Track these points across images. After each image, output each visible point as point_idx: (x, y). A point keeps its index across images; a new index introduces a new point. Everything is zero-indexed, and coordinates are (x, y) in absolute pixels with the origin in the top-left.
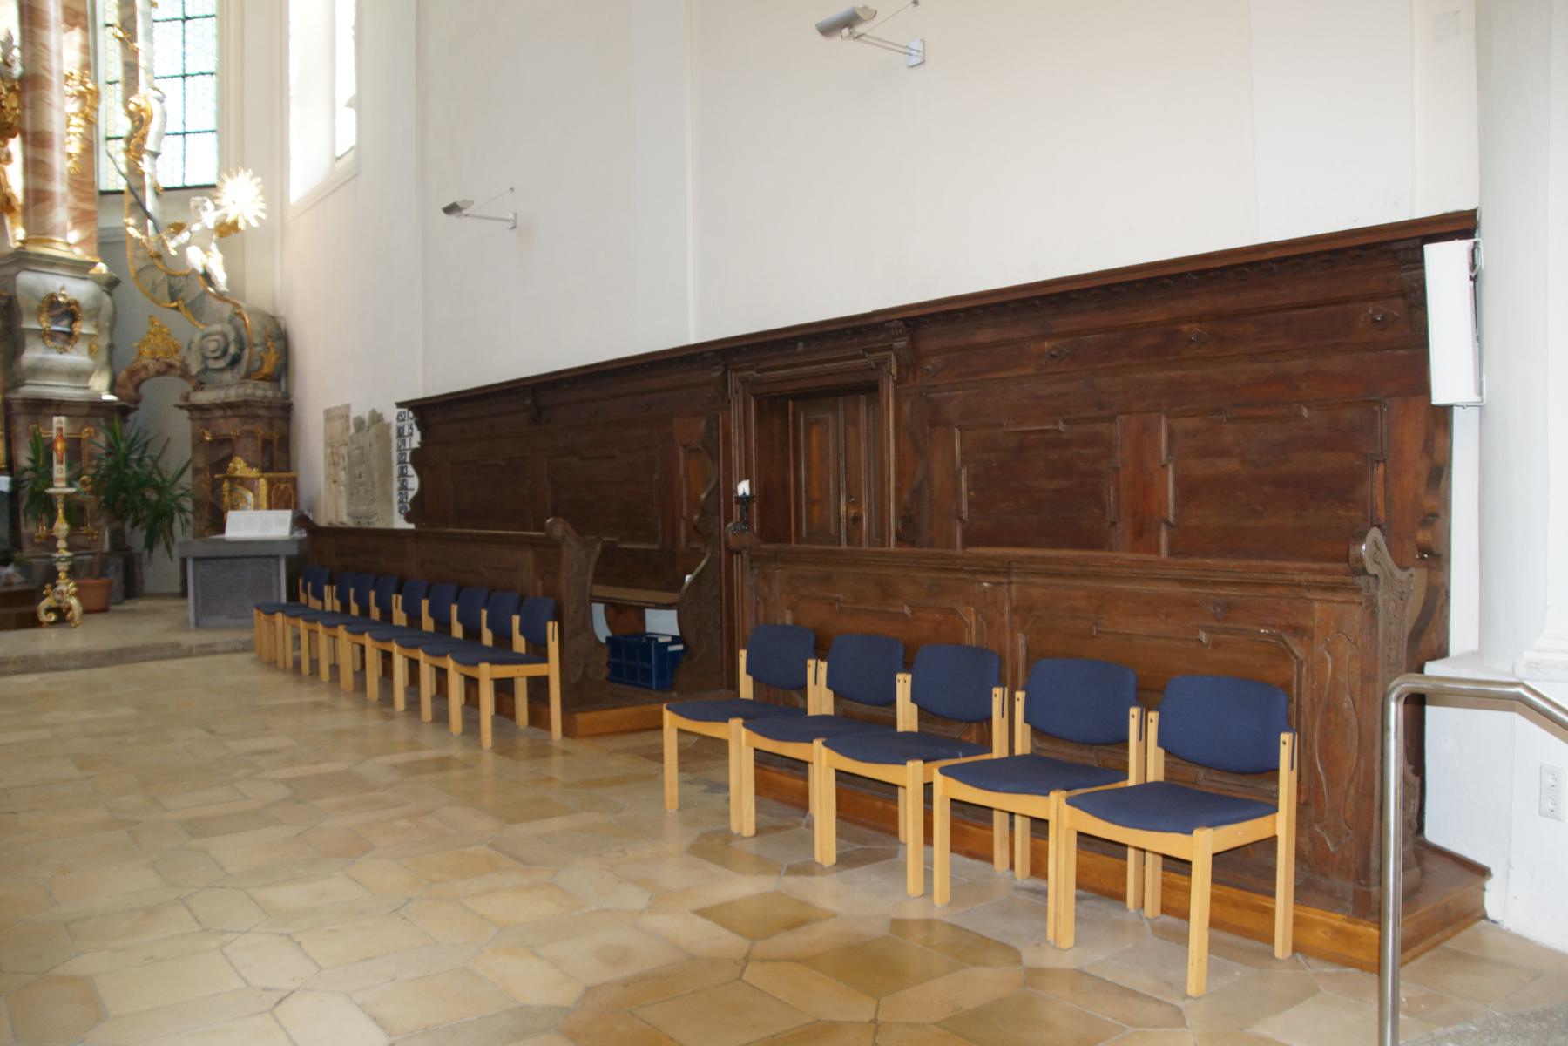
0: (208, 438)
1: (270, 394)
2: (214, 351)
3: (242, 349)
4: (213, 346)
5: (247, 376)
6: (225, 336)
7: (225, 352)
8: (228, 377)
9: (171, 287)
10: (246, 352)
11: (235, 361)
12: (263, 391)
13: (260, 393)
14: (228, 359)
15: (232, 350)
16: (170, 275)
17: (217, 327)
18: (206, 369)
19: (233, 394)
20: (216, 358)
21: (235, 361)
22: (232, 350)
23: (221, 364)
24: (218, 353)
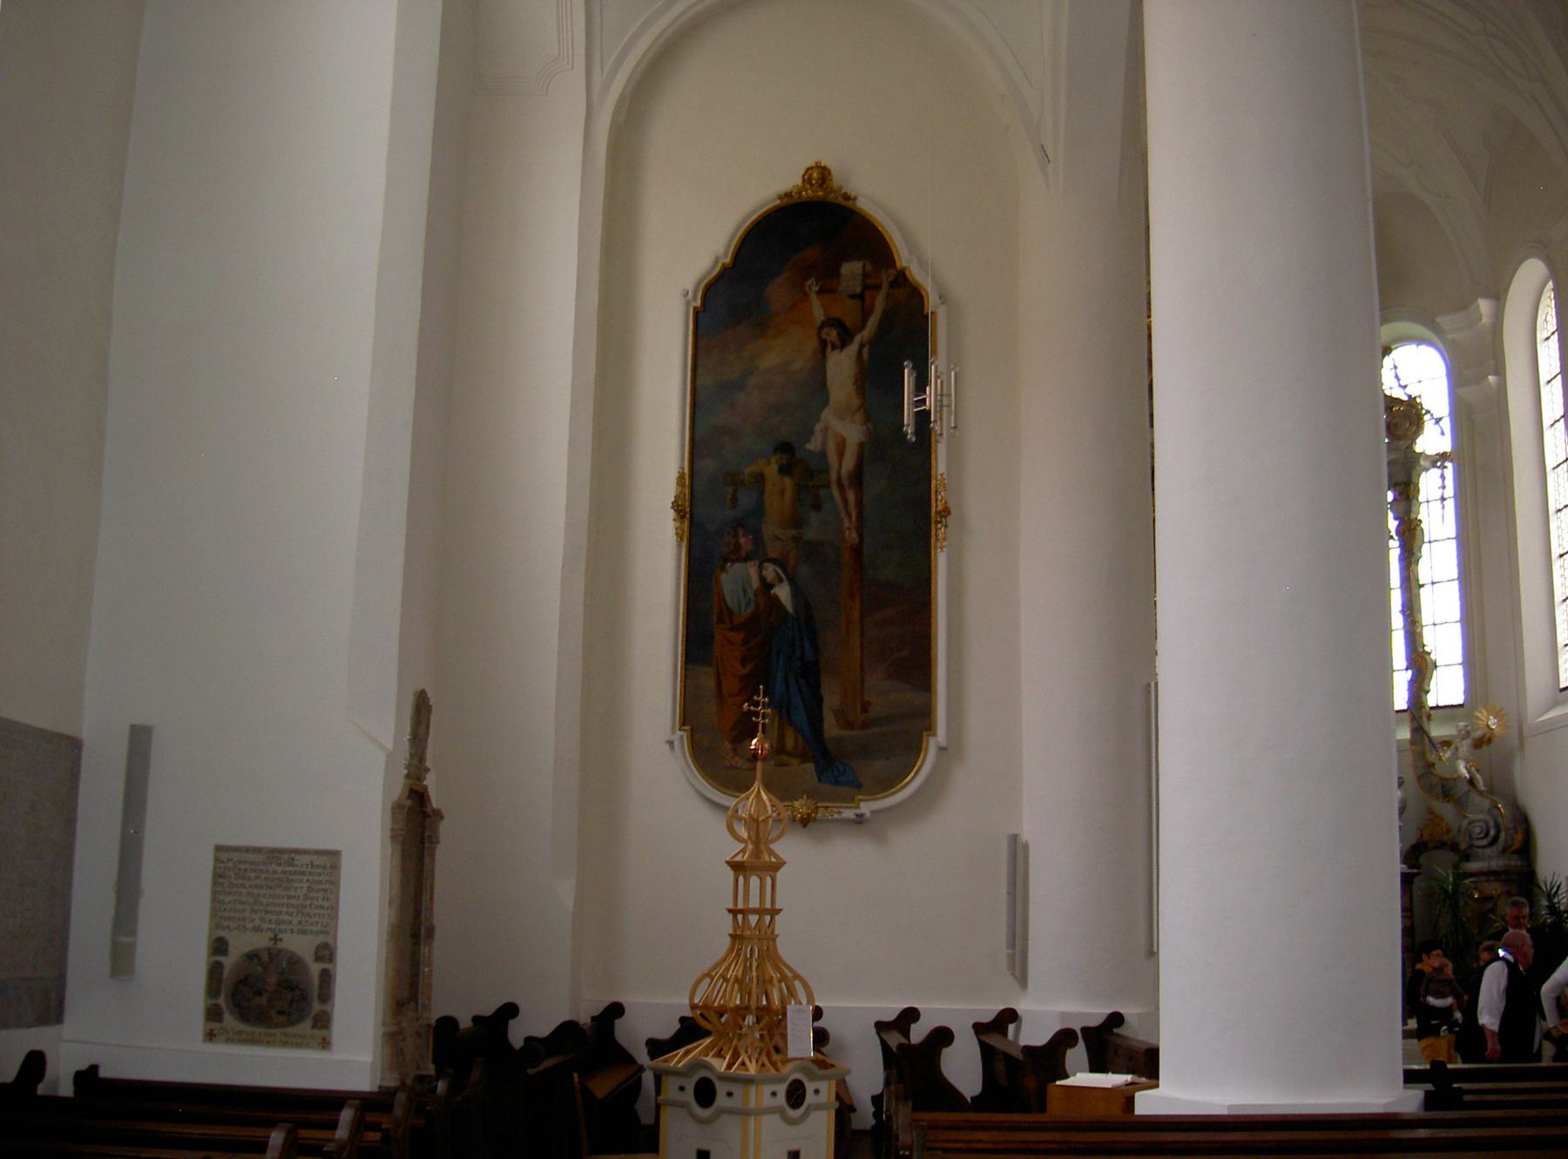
0: (1476, 896)
1: (1519, 863)
2: (1480, 833)
3: (1498, 831)
4: (1478, 830)
5: (1504, 851)
6: (1486, 823)
7: (1487, 834)
8: (1488, 851)
9: (1443, 786)
10: (1503, 835)
11: (1495, 840)
12: (1516, 862)
13: (1513, 863)
14: (1489, 839)
15: (1492, 833)
16: (1441, 779)
17: (1480, 816)
18: (1471, 846)
19: (1495, 864)
20: (1479, 839)
21: (1495, 840)
22: (1492, 833)
23: (1484, 842)
24: (1482, 835)
